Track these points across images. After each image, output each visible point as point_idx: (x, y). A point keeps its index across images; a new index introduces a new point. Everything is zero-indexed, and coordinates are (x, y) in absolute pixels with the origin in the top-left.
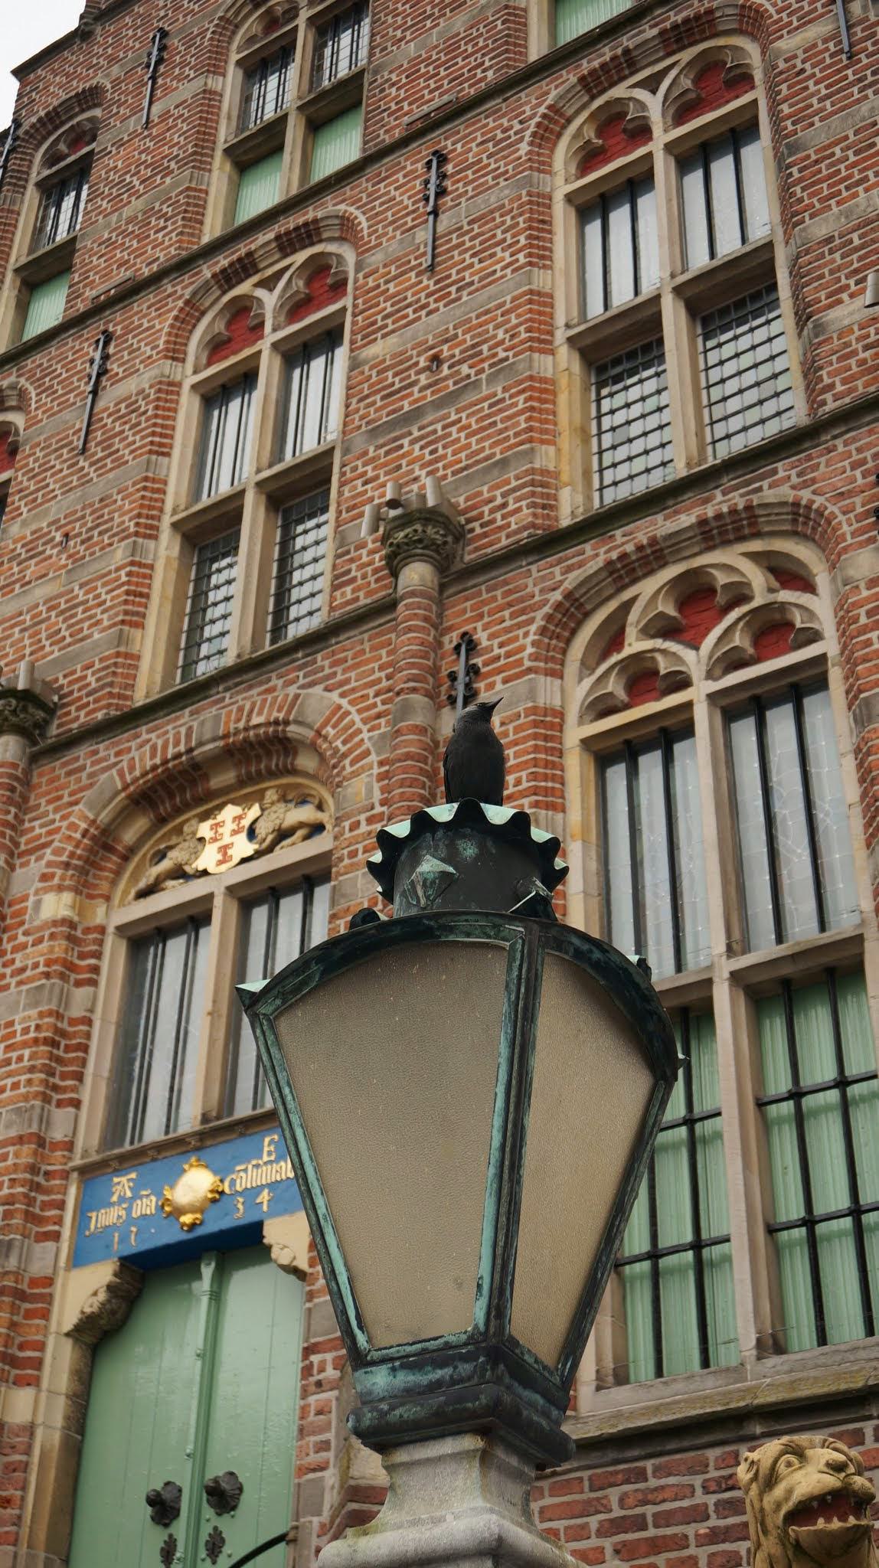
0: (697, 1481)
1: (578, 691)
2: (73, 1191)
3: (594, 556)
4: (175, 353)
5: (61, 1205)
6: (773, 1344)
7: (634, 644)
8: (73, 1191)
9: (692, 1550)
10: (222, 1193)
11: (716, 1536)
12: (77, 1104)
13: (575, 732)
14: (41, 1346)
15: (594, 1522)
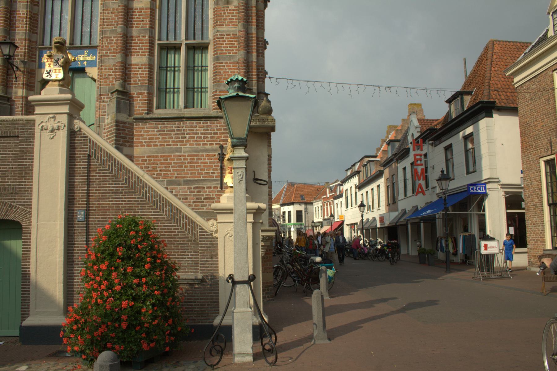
0: (174, 126)
2: (38, 52)
5: (36, 55)
6: (186, 107)
8: (38, 52)
9: (172, 136)
10: (75, 60)
11: (176, 134)
12: (37, 33)
14: (34, 84)
15: (156, 130)
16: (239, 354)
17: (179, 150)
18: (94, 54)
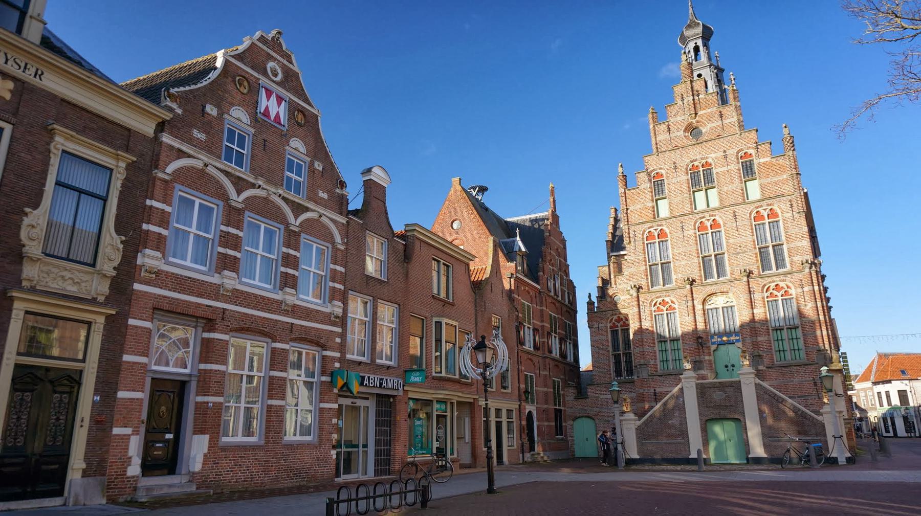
1: (766, 295)
3: (767, 280)
4: (695, 229)
7: (772, 291)
13: (766, 300)
16: (841, 462)
17: (792, 381)
18: (738, 336)
